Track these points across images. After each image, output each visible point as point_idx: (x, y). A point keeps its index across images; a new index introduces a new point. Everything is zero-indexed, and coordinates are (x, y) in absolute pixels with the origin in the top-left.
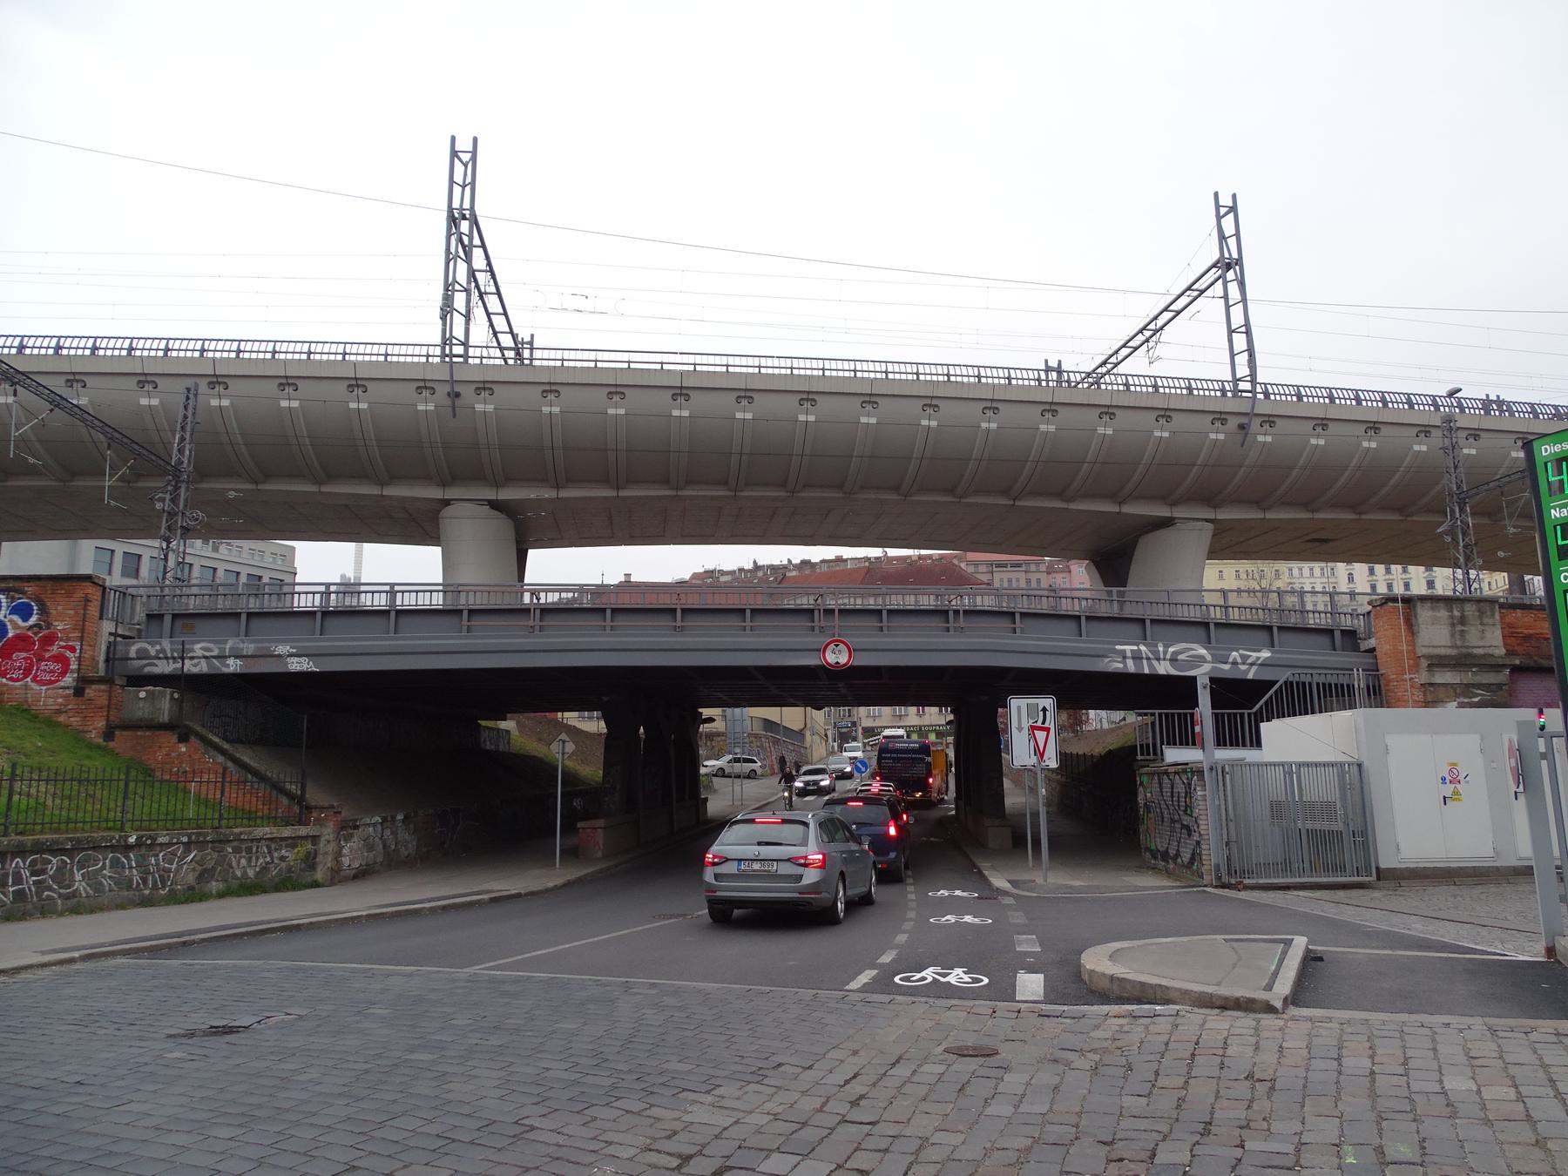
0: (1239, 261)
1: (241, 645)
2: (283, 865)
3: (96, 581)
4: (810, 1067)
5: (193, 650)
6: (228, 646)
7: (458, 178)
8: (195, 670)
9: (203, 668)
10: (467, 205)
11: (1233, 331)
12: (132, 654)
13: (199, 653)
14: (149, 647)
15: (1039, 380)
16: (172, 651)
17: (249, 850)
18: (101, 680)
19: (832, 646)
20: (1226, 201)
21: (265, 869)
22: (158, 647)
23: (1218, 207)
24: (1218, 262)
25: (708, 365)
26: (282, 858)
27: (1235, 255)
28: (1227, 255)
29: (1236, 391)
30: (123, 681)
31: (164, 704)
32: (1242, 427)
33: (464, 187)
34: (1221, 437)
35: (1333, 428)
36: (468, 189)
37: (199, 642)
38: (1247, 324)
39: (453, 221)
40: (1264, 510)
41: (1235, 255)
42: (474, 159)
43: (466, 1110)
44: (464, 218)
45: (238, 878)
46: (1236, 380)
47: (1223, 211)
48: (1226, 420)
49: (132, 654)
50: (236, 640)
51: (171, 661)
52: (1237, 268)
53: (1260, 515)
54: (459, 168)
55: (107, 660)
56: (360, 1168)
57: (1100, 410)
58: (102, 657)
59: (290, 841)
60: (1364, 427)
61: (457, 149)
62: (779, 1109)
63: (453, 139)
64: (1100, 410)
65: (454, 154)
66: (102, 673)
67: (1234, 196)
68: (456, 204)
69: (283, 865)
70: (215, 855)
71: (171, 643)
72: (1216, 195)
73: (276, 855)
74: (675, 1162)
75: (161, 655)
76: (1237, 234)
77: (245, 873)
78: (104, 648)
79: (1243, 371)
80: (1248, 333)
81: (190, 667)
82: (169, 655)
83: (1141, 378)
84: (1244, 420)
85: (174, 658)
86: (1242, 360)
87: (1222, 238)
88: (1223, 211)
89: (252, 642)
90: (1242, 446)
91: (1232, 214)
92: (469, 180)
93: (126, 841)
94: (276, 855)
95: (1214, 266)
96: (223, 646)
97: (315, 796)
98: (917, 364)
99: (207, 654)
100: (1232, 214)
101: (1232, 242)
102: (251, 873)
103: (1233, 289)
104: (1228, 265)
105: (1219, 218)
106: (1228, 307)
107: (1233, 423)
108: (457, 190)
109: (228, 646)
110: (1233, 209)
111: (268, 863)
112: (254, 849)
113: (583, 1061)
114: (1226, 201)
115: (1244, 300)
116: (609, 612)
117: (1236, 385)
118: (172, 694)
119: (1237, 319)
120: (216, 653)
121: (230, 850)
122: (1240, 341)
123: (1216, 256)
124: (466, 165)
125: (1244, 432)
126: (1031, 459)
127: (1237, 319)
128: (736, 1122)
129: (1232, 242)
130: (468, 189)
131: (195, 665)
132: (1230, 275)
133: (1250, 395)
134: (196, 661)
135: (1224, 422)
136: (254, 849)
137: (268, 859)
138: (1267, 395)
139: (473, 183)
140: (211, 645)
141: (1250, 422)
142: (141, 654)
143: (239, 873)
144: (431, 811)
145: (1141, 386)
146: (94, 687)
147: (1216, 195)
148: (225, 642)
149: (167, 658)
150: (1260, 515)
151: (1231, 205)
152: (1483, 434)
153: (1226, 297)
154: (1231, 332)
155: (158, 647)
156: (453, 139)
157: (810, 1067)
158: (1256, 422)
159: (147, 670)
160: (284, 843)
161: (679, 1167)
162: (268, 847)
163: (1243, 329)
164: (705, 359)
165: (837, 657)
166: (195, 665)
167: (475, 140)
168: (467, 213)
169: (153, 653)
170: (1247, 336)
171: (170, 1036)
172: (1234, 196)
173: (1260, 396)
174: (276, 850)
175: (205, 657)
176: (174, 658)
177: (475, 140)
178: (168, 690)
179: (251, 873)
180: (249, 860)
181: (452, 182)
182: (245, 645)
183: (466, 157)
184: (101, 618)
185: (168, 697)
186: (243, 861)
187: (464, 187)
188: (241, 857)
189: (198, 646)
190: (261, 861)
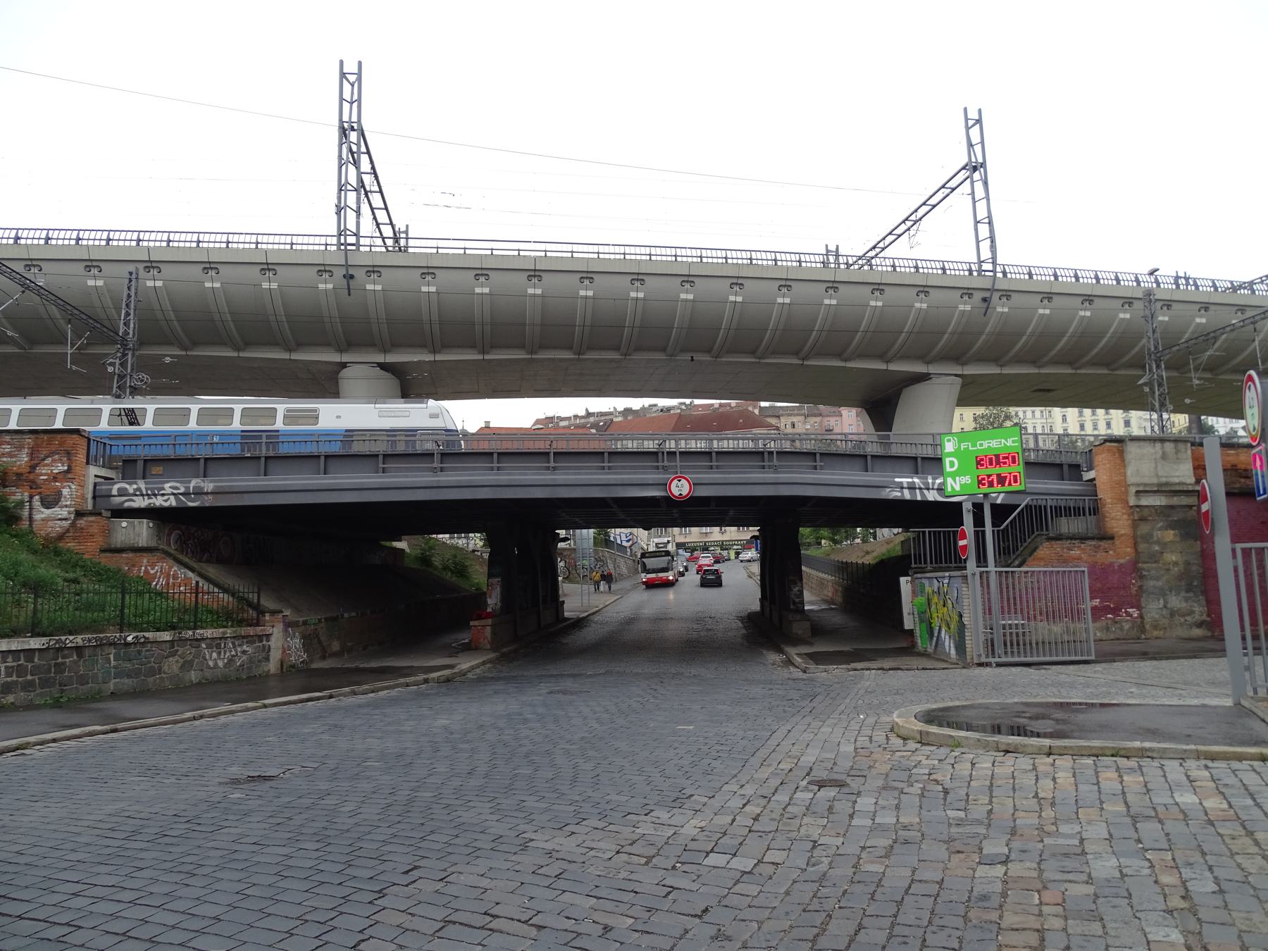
0: (983, 165)
1: (202, 484)
2: (245, 657)
3: (84, 434)
4: (713, 797)
5: (164, 489)
6: (192, 485)
7: (347, 96)
8: (166, 504)
9: (172, 502)
10: (354, 118)
11: (979, 222)
12: (115, 492)
13: (169, 491)
14: (127, 486)
15: (970, 271)
16: (147, 489)
17: (218, 646)
18: (91, 514)
19: (676, 481)
20: (973, 115)
21: (231, 661)
22: (135, 486)
23: (967, 119)
24: (967, 165)
25: (610, 253)
26: (244, 652)
28: (973, 160)
29: (980, 271)
30: (109, 514)
31: (141, 531)
32: (984, 300)
33: (351, 103)
34: (968, 308)
35: (1098, 303)
36: (355, 105)
37: (168, 482)
38: (990, 217)
39: (344, 132)
40: (1040, 367)
41: (980, 160)
42: (359, 79)
43: (478, 829)
44: (352, 129)
45: (211, 668)
46: (980, 262)
47: (971, 123)
48: (1051, 298)
49: (115, 492)
50: (198, 480)
51: (146, 498)
52: (982, 170)
53: (1036, 371)
54: (347, 87)
55: (94, 497)
56: (420, 867)
57: (961, 292)
58: (90, 496)
59: (250, 639)
60: (1081, 299)
61: (345, 71)
62: (703, 824)
63: (341, 62)
64: (961, 292)
65: (343, 75)
66: (90, 507)
67: (980, 111)
68: (346, 118)
69: (245, 657)
70: (193, 650)
71: (146, 483)
72: (965, 109)
73: (239, 649)
74: (643, 860)
75: (138, 493)
76: (982, 142)
77: (216, 664)
78: (91, 487)
79: (986, 254)
80: (990, 223)
81: (159, 502)
82: (145, 493)
83: (955, 264)
84: (987, 295)
85: (148, 495)
86: (985, 246)
87: (970, 145)
88: (971, 123)
89: (211, 482)
90: (985, 315)
91: (978, 125)
92: (355, 97)
93: (125, 639)
94: (239, 649)
95: (964, 168)
96: (188, 485)
97: (267, 603)
98: (847, 256)
99: (175, 492)
100: (978, 125)
101: (978, 149)
102: (221, 664)
103: (979, 187)
104: (974, 167)
105: (968, 128)
106: (974, 202)
107: (978, 296)
108: (346, 106)
109: (192, 485)
110: (979, 121)
111: (233, 656)
112: (223, 645)
113: (547, 795)
114: (973, 115)
115: (987, 198)
116: (495, 455)
118: (148, 523)
119: (982, 214)
120: (182, 490)
121: (204, 646)
122: (984, 230)
123: (965, 160)
124: (352, 85)
125: (985, 305)
126: (906, 330)
127: (982, 214)
128: (675, 833)
129: (978, 149)
130: (355, 105)
131: (166, 501)
132: (976, 176)
133: (991, 274)
134: (166, 497)
135: (970, 295)
136: (223, 645)
137: (233, 653)
138: (1004, 273)
139: (359, 100)
140: (178, 485)
141: (991, 296)
142: (122, 493)
143: (211, 664)
144: (353, 614)
145: (932, 268)
146: (85, 518)
147: (965, 109)
148: (190, 482)
149: (142, 495)
150: (1036, 371)
151: (977, 118)
152: (1212, 307)
153: (973, 193)
154: (977, 222)
155: (135, 486)
156: (341, 62)
157: (713, 797)
158: (996, 296)
159: (127, 505)
160: (245, 640)
161: (647, 864)
162: (233, 644)
163: (987, 220)
164: (581, 248)
165: (680, 488)
166: (166, 501)
167: (360, 63)
168: (355, 126)
169: (131, 491)
170: (990, 226)
171: (220, 783)
172: (980, 111)
173: (1000, 275)
174: (239, 645)
175: (173, 494)
176: (148, 495)
177: (360, 63)
178: (145, 521)
179: (221, 664)
180: (219, 653)
181: (342, 99)
182: (206, 484)
183: (352, 78)
184: (88, 463)
185: (145, 525)
186: (215, 655)
187: (351, 103)
188: (212, 652)
189: (167, 486)
190: (228, 654)
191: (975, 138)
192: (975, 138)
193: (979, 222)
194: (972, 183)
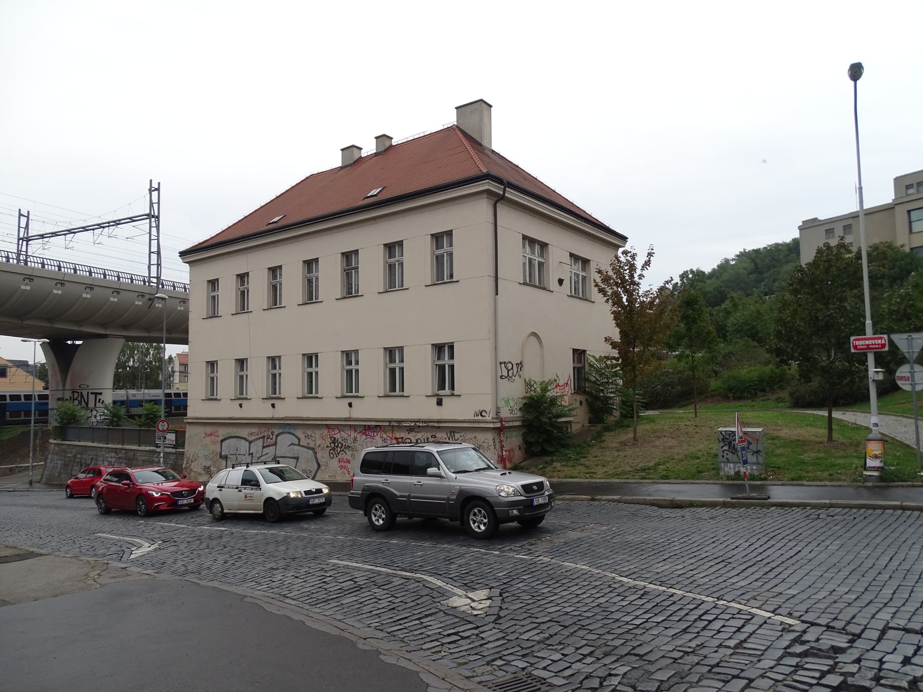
0: (158, 217)
11: (152, 253)
20: (155, 185)
27: (156, 214)
28: (153, 214)
29: (149, 282)
32: (150, 299)
41: (156, 214)
46: (150, 277)
67: (159, 183)
72: (151, 181)
76: (159, 203)
79: (154, 274)
86: (154, 269)
87: (151, 204)
88: (153, 189)
100: (157, 192)
101: (156, 206)
103: (154, 230)
106: (150, 240)
110: (158, 189)
114: (155, 185)
117: (149, 279)
119: (154, 249)
123: (148, 212)
133: (155, 285)
138: (163, 287)
147: (151, 181)
151: (157, 187)
153: (150, 233)
154: (150, 252)
172: (159, 183)
173: (160, 286)
191: (155, 200)
192: (155, 200)
193: (152, 253)
194: (151, 227)
